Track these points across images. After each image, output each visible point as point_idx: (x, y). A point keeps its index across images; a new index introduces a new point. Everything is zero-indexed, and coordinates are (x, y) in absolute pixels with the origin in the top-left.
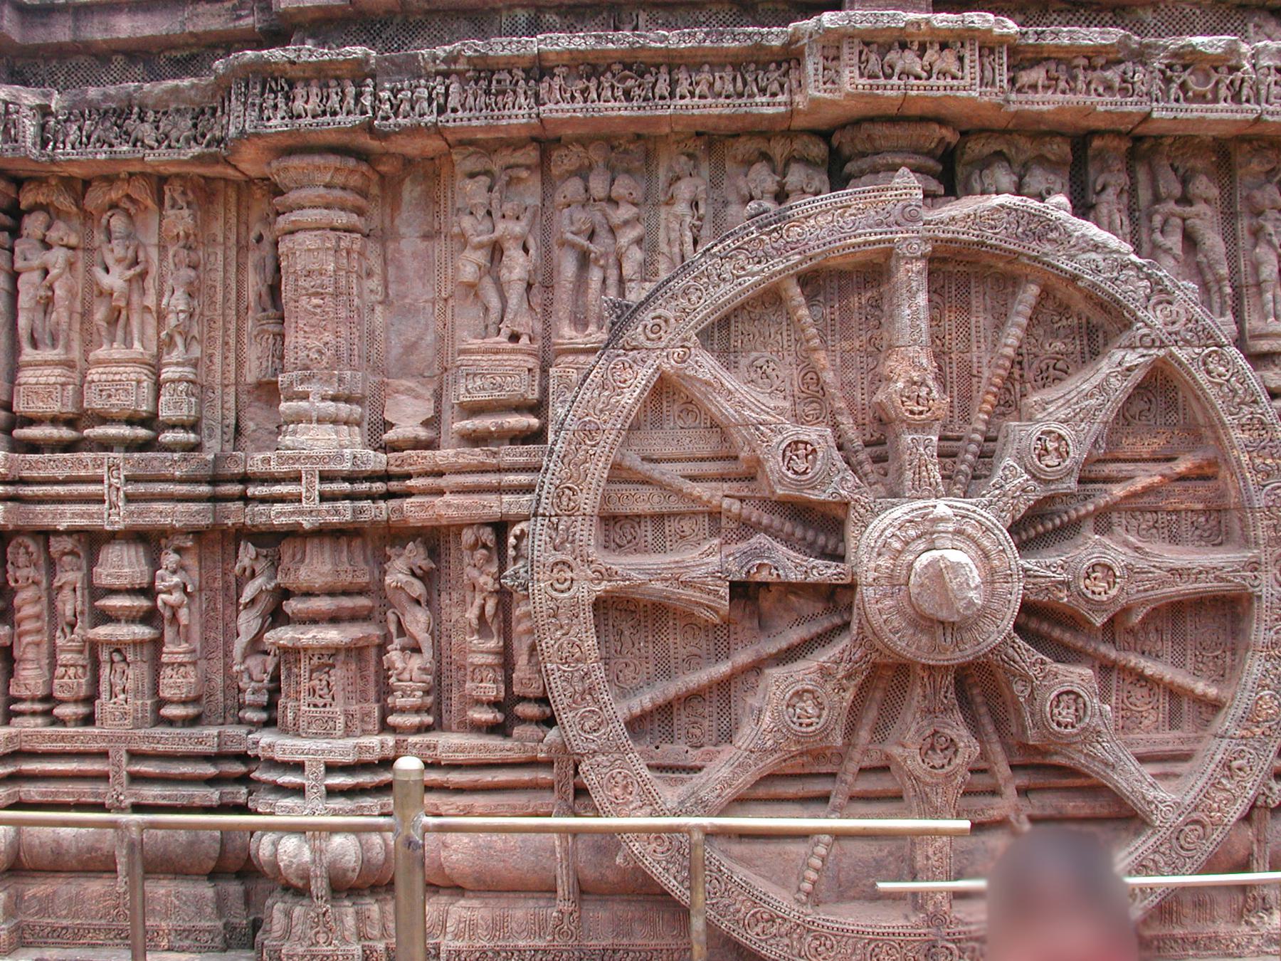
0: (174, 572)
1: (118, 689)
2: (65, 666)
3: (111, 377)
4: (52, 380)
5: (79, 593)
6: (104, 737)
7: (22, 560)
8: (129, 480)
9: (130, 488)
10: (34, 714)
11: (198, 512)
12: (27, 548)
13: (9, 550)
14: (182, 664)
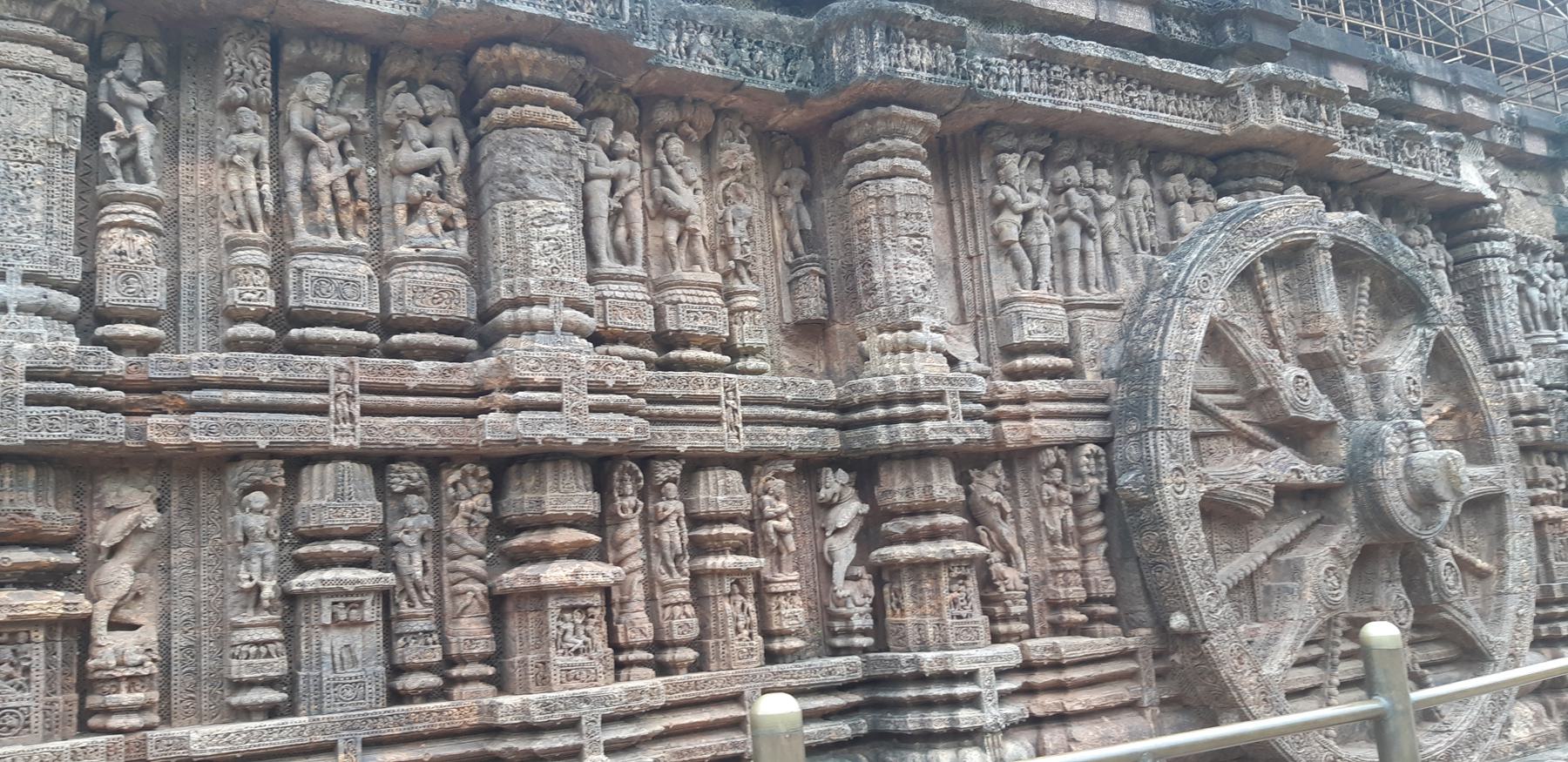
1: (741, 624)
3: (697, 300)
4: (640, 296)
7: (629, 488)
11: (810, 436)
13: (616, 475)
14: (793, 593)
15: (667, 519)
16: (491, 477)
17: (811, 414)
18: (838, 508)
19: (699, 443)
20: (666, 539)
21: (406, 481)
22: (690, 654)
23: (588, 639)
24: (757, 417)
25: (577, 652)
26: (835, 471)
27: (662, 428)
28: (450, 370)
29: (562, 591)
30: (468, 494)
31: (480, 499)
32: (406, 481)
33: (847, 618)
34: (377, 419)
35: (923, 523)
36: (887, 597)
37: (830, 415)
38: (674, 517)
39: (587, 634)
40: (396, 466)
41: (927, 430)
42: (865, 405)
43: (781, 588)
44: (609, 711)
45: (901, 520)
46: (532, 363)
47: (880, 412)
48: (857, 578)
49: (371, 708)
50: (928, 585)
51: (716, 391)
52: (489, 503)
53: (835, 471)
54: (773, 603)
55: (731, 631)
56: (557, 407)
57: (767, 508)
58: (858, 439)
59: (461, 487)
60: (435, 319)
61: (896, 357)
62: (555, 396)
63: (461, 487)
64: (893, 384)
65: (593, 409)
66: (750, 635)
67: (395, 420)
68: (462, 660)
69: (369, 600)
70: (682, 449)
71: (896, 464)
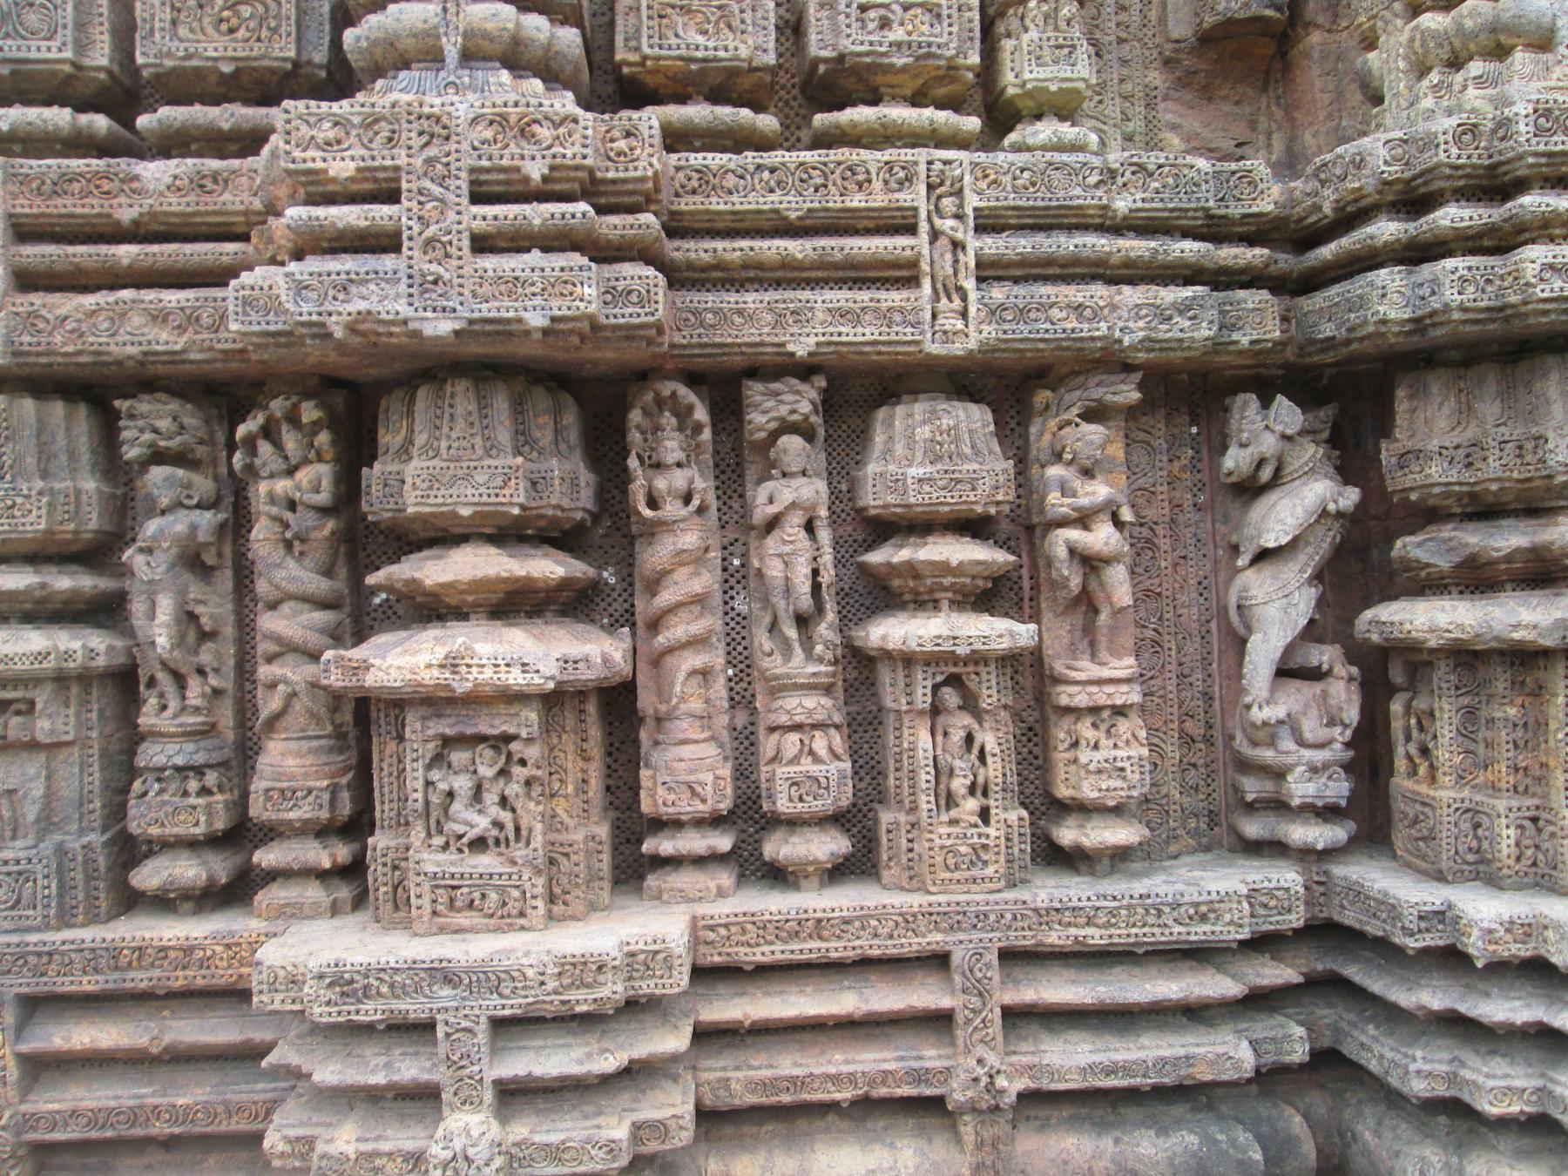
0: (1088, 473)
1: (959, 785)
2: (798, 727)
5: (824, 535)
6: (934, 917)
7: (672, 447)
8: (987, 224)
9: (993, 245)
10: (700, 861)
11: (1183, 308)
12: (683, 414)
13: (635, 416)
14: (1120, 711)
15: (773, 524)
16: (332, 422)
17: (1188, 249)
18: (1272, 497)
19: (849, 333)
20: (775, 570)
21: (148, 436)
22: (827, 846)
23: (506, 817)
24: (1023, 262)
25: (479, 844)
26: (1266, 403)
27: (750, 297)
28: (215, 177)
29: (435, 702)
30: (277, 464)
31: (304, 476)
32: (148, 436)
33: (1279, 774)
34: (56, 298)
35: (1509, 539)
36: (1397, 725)
37: (1254, 255)
38: (797, 519)
39: (504, 802)
40: (121, 404)
41: (1530, 271)
42: (1352, 217)
43: (1081, 698)
44: (510, 1006)
45: (1447, 531)
46: (327, 132)
47: (1386, 229)
48: (1314, 674)
49: (47, 927)
50: (1512, 711)
51: (904, 198)
52: (326, 484)
53: (1266, 403)
54: (1061, 733)
55: (925, 802)
56: (385, 242)
57: (1054, 497)
58: (1329, 313)
59: (265, 448)
60: (227, 68)
61: (1458, 78)
62: (382, 213)
63: (265, 448)
64: (1430, 142)
65: (482, 244)
66: (984, 814)
67: (89, 300)
68: (271, 833)
69: (42, 697)
70: (801, 346)
71: (1436, 383)
